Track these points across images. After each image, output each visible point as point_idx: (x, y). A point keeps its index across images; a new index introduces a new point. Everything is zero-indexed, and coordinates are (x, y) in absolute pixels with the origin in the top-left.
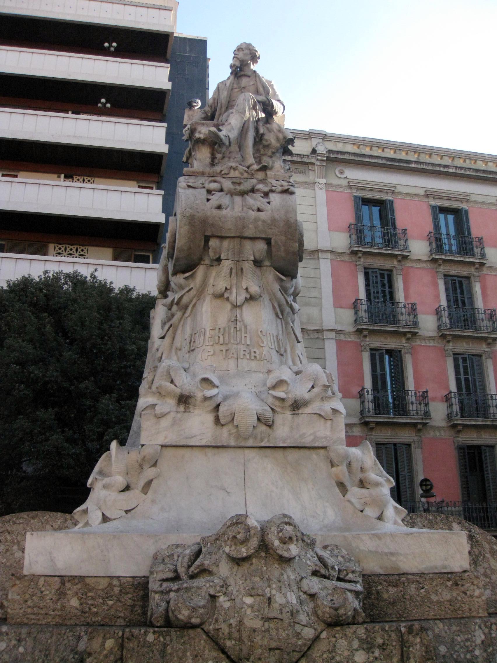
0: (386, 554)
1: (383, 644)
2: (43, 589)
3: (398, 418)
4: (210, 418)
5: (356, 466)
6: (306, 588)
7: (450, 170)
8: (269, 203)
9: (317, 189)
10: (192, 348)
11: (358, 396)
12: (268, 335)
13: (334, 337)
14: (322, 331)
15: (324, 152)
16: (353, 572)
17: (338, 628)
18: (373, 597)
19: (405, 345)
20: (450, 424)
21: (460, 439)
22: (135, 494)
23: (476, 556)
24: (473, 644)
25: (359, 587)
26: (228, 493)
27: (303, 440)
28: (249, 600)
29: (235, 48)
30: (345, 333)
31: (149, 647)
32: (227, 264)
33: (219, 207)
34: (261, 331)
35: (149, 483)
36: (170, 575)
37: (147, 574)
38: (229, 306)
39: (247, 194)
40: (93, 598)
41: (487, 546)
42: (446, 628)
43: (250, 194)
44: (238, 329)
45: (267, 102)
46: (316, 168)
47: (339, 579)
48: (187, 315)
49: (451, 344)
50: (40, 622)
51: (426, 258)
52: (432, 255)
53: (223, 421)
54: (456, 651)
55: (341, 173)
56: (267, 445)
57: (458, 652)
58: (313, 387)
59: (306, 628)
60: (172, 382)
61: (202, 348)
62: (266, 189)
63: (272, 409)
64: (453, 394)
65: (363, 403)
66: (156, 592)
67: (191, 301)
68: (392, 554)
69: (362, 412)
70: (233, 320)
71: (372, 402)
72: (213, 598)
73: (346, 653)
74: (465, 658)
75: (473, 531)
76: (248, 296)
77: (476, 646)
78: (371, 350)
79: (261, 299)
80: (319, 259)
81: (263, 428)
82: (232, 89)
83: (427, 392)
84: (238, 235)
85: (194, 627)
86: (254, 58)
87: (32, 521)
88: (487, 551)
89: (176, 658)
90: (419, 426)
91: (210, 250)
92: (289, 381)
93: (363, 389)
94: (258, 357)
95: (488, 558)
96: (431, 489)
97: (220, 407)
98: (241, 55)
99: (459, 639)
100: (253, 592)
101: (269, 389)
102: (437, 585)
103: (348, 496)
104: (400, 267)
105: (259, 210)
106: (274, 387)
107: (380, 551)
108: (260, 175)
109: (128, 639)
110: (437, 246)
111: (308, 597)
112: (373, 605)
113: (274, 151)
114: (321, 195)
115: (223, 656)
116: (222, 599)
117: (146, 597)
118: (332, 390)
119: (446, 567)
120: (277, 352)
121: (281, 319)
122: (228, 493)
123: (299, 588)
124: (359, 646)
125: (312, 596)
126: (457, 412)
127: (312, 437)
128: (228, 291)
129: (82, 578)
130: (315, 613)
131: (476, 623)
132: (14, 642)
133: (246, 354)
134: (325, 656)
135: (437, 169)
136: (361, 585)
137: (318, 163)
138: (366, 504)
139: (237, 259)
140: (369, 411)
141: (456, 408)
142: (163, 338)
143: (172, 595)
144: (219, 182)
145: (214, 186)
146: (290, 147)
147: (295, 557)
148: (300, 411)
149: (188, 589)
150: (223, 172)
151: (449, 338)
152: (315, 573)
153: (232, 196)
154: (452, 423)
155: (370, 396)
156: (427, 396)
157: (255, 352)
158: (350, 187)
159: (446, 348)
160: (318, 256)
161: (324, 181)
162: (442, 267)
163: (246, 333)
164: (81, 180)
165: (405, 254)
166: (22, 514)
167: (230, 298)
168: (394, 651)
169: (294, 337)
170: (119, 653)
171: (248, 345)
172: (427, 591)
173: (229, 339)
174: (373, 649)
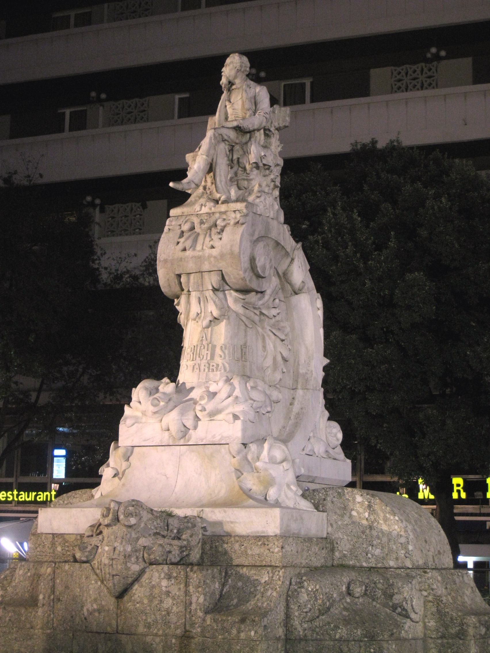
1: (176, 577)
8: (221, 239)
18: (213, 549)
27: (214, 440)
40: (68, 547)
41: (382, 515)
68: (232, 522)
73: (158, 580)
74: (250, 590)
75: (372, 502)
87: (84, 496)
88: (381, 518)
95: (382, 524)
102: (251, 544)
119: (264, 532)
124: (164, 577)
127: (220, 437)
129: (62, 535)
132: (26, 570)
134: (147, 581)
139: (201, 290)
166: (77, 491)
168: (182, 581)
172: (246, 547)
174: (171, 579)
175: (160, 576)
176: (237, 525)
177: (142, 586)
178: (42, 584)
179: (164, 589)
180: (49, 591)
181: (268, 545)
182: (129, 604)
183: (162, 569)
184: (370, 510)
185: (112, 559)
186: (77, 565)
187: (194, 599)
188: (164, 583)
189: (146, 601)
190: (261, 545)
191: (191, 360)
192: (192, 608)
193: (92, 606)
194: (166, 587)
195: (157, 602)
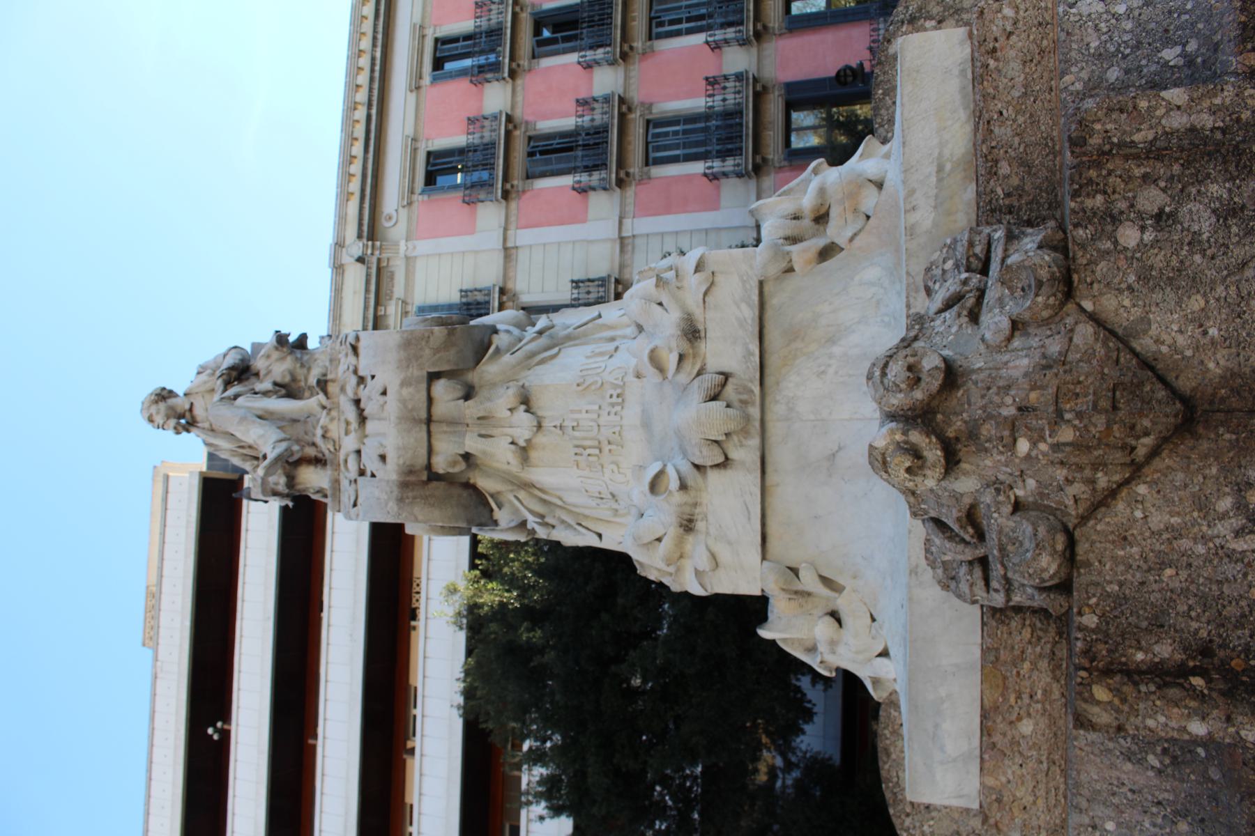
0: (940, 180)
2: (1004, 779)
3: (747, 123)
4: (714, 477)
5: (791, 228)
6: (1001, 337)
7: (378, 54)
9: (414, 254)
10: (610, 497)
11: (716, 182)
12: (585, 373)
13: (630, 220)
14: (622, 239)
15: (361, 245)
16: (971, 244)
17: (1075, 277)
18: (1016, 204)
19: (638, 114)
20: (754, 41)
21: (777, 25)
22: (842, 603)
23: (944, 11)
24: (1105, 16)
25: (999, 234)
26: (840, 448)
27: (750, 321)
28: (1023, 446)
29: (149, 427)
30: (623, 205)
31: (1108, 623)
32: (472, 444)
33: (383, 458)
34: (578, 385)
35: (826, 581)
36: (978, 572)
37: (977, 610)
38: (540, 439)
39: (363, 410)
42: (1074, 69)
43: (362, 405)
44: (575, 424)
45: (225, 377)
46: (384, 256)
47: (984, 271)
48: (559, 503)
49: (635, 45)
50: (1062, 787)
51: (509, 87)
52: (504, 79)
53: (721, 459)
54: (1118, 50)
55: (390, 218)
56: (757, 383)
57: (1119, 45)
58: (660, 304)
59: (1075, 340)
60: (659, 540)
61: (609, 482)
62: (354, 380)
63: (699, 374)
64: (709, 39)
65: (725, 175)
66: (1009, 599)
67: (536, 496)
68: (940, 169)
69: (739, 175)
70: (560, 432)
71: (723, 161)
72: (1017, 506)
75: (902, 16)
76: (523, 407)
77: (1107, 12)
78: (647, 164)
79: (527, 384)
80: (517, 247)
81: (730, 389)
82: (212, 430)
83: (707, 79)
84: (424, 427)
85: (1071, 543)
86: (164, 395)
87: (894, 756)
89: (1129, 577)
90: (759, 88)
91: (451, 470)
92: (651, 346)
93: (705, 175)
94: (619, 391)
96: (850, 68)
97: (696, 462)
98: (159, 419)
99: (1093, 45)
100: (1007, 440)
101: (665, 378)
103: (841, 241)
104: (523, 126)
105: (384, 393)
106: (661, 369)
107: (935, 191)
108: (331, 388)
109: (1092, 661)
110: (490, 71)
111: (1017, 333)
112: (1031, 203)
113: (298, 365)
114: (423, 247)
115: (1124, 493)
116: (1020, 493)
117: (1018, 609)
118: (666, 271)
119: (963, 72)
120: (611, 356)
121: (560, 350)
122: (840, 448)
123: (998, 349)
124: (1109, 239)
125: (1016, 325)
126: (736, 32)
127: (744, 306)
128: (516, 441)
129: (984, 716)
130: (1046, 322)
131: (1066, 13)
133: (613, 410)
135: (377, 74)
136: (995, 231)
137: (377, 253)
138: (855, 211)
140: (738, 165)
141: (730, 33)
142: (600, 536)
143: (1015, 577)
144: (347, 455)
145: (353, 466)
146: (292, 339)
147: (945, 360)
148: (701, 327)
149: (1002, 549)
150: (332, 449)
151: (626, 48)
152: (974, 317)
153: (366, 436)
154: (752, 38)
155: (715, 164)
156: (714, 77)
157: (611, 396)
158: (410, 204)
159: (640, 51)
160: (513, 248)
161: (402, 243)
162: (521, 62)
163: (580, 412)
164: (417, 596)
165: (504, 119)
166: (883, 773)
167: (527, 437)
169: (590, 325)
170: (1118, 678)
171: (600, 407)
173: (592, 439)
175: (1108, 252)
176: (947, 152)
177: (1145, 321)
178: (1150, 723)
179: (1149, 236)
180: (1173, 692)
181: (996, 40)
182: (1211, 365)
183: (1083, 246)
184: (919, 18)
185: (1059, 413)
186: (1082, 579)
187: (1178, 121)
188: (1129, 236)
189: (1196, 303)
190: (997, 60)
191: (597, 451)
192: (1209, 125)
193: (1224, 516)
194: (1143, 229)
195: (1197, 258)
